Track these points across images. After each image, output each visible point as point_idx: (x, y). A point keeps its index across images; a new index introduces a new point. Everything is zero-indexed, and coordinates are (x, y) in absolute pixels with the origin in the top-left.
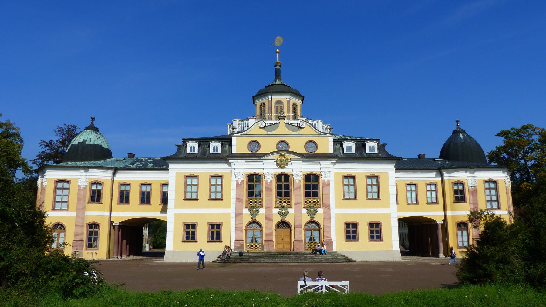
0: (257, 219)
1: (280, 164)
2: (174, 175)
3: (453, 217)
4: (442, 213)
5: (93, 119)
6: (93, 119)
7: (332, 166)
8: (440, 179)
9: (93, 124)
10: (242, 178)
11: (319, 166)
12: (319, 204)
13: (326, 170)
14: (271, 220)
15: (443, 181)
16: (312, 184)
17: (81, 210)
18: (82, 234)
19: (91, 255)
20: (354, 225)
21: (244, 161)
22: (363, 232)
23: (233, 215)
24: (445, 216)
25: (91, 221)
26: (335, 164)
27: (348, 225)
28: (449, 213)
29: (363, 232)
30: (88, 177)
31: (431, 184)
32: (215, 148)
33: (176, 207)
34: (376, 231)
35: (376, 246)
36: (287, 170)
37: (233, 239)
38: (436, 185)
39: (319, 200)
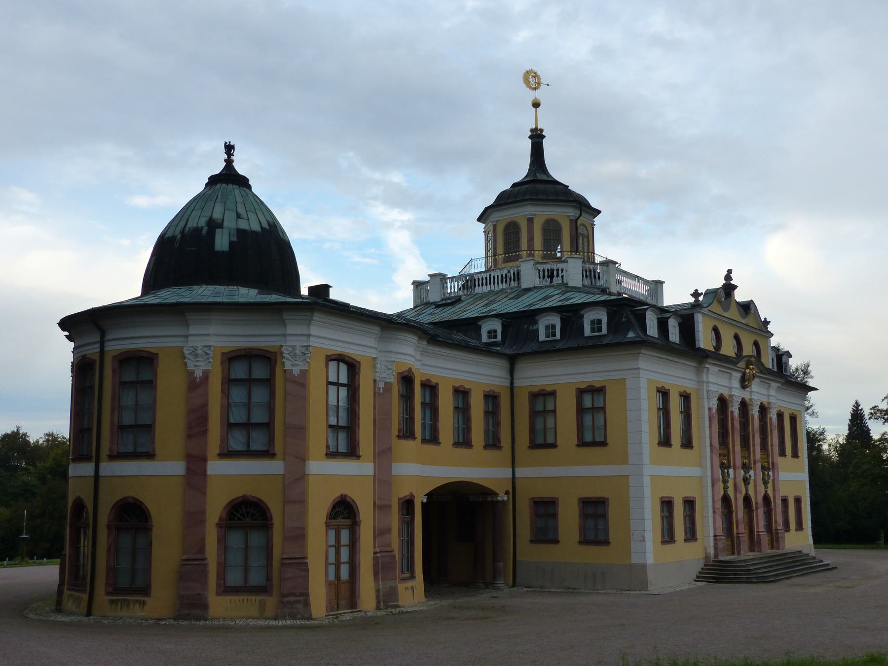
1: (744, 382)
5: (229, 149)
6: (229, 149)
9: (229, 162)
10: (714, 404)
12: (768, 462)
14: (741, 493)
17: (383, 455)
18: (389, 530)
19: (410, 591)
21: (716, 369)
25: (404, 493)
30: (393, 357)
36: (746, 394)
37: (712, 534)
39: (768, 455)
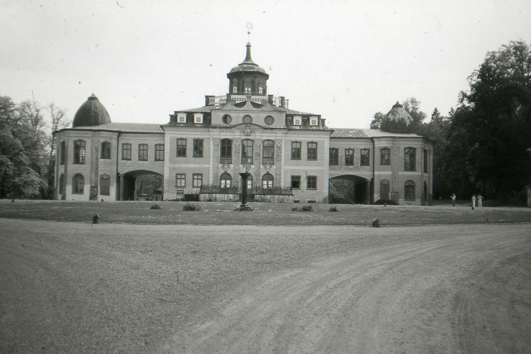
0: (228, 172)
2: (169, 138)
3: (380, 176)
4: (372, 173)
7: (284, 135)
8: (372, 146)
11: (274, 135)
13: (280, 138)
15: (374, 147)
16: (270, 147)
20: (299, 177)
22: (304, 183)
23: (211, 169)
24: (374, 175)
26: (286, 133)
27: (293, 177)
28: (376, 173)
29: (304, 183)
31: (365, 149)
32: (199, 119)
33: (170, 163)
34: (312, 182)
35: (312, 192)
38: (369, 150)
